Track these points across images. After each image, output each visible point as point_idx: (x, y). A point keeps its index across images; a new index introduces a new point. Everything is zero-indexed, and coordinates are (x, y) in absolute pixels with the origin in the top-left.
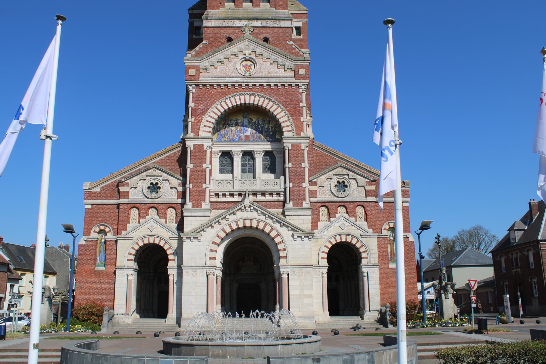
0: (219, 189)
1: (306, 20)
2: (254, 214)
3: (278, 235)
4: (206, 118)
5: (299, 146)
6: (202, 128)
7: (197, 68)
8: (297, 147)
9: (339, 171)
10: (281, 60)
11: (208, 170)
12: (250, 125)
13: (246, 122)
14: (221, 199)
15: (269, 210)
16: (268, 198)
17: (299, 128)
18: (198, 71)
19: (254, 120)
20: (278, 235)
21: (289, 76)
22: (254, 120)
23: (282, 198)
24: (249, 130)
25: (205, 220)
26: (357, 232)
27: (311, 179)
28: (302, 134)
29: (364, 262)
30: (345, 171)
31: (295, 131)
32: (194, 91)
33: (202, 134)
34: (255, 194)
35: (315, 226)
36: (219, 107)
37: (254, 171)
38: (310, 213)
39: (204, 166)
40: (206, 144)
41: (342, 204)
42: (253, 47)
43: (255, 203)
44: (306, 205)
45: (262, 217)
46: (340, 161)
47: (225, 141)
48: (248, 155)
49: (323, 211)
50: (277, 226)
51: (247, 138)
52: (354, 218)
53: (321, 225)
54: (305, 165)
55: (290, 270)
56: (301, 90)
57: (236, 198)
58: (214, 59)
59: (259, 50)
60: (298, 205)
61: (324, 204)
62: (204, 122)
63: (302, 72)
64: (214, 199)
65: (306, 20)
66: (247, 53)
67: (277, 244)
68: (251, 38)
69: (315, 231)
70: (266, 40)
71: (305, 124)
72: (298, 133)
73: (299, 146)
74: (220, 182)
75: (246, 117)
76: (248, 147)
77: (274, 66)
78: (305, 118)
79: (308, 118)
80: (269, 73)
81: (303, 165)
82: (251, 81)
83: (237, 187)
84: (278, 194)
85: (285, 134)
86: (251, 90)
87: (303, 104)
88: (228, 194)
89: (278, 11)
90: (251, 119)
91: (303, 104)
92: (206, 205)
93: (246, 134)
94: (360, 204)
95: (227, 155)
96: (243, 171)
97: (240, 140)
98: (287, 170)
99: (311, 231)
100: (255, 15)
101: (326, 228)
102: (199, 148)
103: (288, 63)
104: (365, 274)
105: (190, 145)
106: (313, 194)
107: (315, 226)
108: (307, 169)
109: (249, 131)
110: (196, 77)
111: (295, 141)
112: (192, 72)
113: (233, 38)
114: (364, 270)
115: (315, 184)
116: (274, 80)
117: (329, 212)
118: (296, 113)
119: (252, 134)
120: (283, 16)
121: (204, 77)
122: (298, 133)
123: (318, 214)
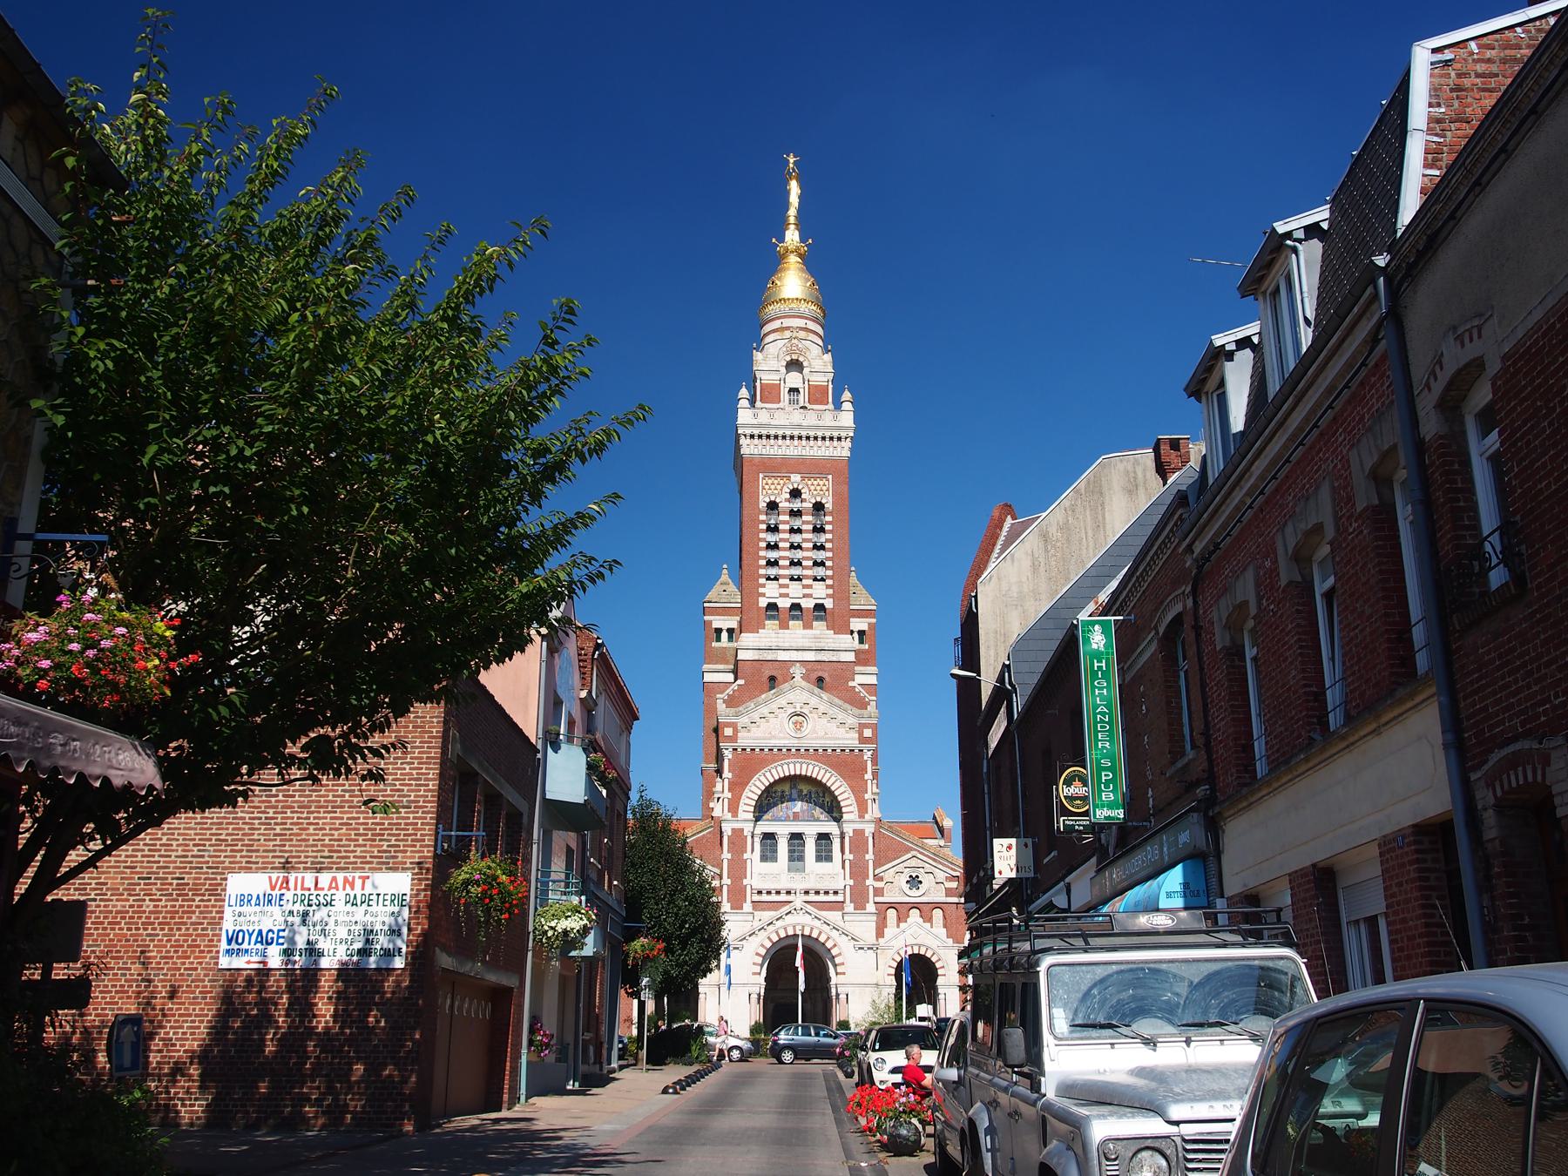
0: (765, 886)
1: (874, 620)
2: (807, 919)
3: (835, 945)
4: (747, 793)
5: (863, 831)
6: (742, 807)
7: (734, 726)
8: (859, 833)
9: (913, 862)
10: (841, 716)
11: (749, 861)
12: (801, 798)
13: (795, 795)
14: (765, 897)
15: (824, 913)
16: (822, 898)
17: (862, 808)
18: (736, 731)
19: (805, 792)
20: (835, 945)
21: (850, 739)
22: (805, 792)
23: (839, 898)
24: (799, 804)
25: (747, 928)
26: (933, 943)
27: (876, 872)
28: (867, 817)
29: (940, 981)
30: (921, 864)
31: (857, 813)
32: (730, 756)
33: (742, 815)
34: (807, 893)
35: (880, 933)
36: (763, 778)
37: (801, 858)
38: (875, 918)
39: (745, 856)
40: (748, 828)
41: (915, 906)
42: (805, 696)
43: (806, 905)
44: (871, 907)
45: (817, 923)
46: (915, 850)
47: (768, 820)
48: (796, 837)
49: (892, 913)
50: (834, 934)
51: (796, 817)
52: (929, 924)
53: (890, 931)
54: (870, 856)
55: (849, 990)
56: (865, 758)
57: (783, 897)
58: (755, 716)
59: (814, 701)
60: (860, 904)
61: (892, 905)
62: (744, 800)
63: (868, 733)
64: (756, 898)
65: (874, 620)
66: (798, 706)
67: (833, 957)
68: (804, 684)
69: (881, 941)
70: (820, 681)
71: (870, 801)
72: (862, 816)
73: (863, 831)
74: (763, 876)
75: (795, 787)
76: (797, 828)
77: (832, 726)
78: (872, 788)
79: (875, 790)
80: (826, 734)
81: (867, 857)
82: (805, 743)
83: (784, 884)
84: (836, 893)
85: (845, 817)
86: (802, 756)
87: (868, 776)
88: (773, 892)
89: (837, 636)
90: (801, 791)
91: (868, 776)
92: (747, 907)
93: (795, 810)
94: (937, 905)
95: (769, 837)
96: (791, 859)
97: (787, 819)
98: (847, 863)
99: (875, 942)
100: (807, 644)
101: (896, 937)
102: (738, 833)
103: (852, 721)
104: (941, 997)
105: (727, 829)
106: (879, 892)
107: (880, 933)
108: (871, 863)
109: (799, 806)
110: (734, 738)
111: (859, 826)
112: (728, 732)
113: (779, 678)
114: (940, 991)
115: (881, 879)
116: (830, 743)
117: (898, 916)
118: (858, 791)
119: (803, 811)
120: (843, 646)
121: (745, 740)
122: (862, 816)
123: (885, 918)
